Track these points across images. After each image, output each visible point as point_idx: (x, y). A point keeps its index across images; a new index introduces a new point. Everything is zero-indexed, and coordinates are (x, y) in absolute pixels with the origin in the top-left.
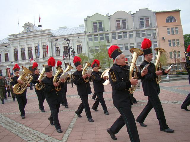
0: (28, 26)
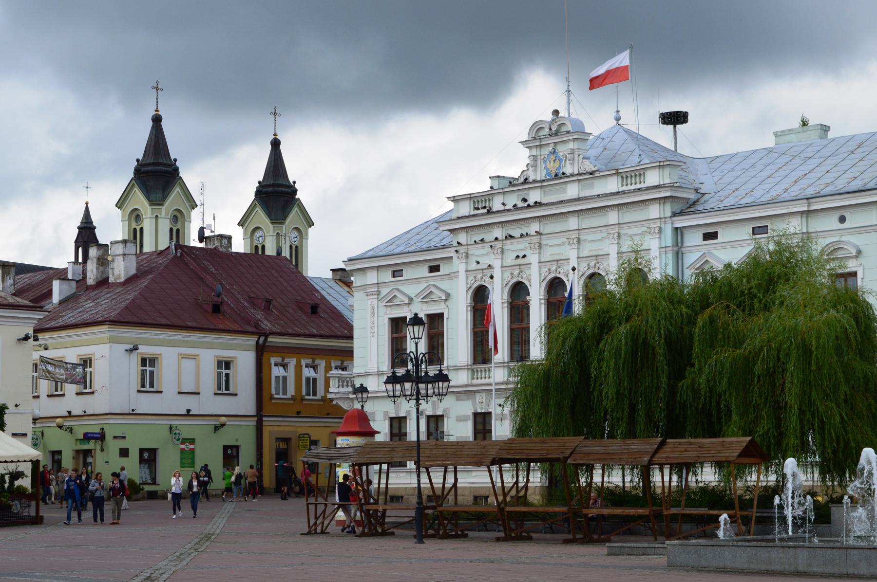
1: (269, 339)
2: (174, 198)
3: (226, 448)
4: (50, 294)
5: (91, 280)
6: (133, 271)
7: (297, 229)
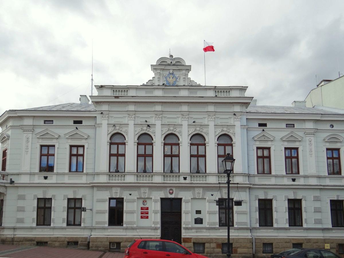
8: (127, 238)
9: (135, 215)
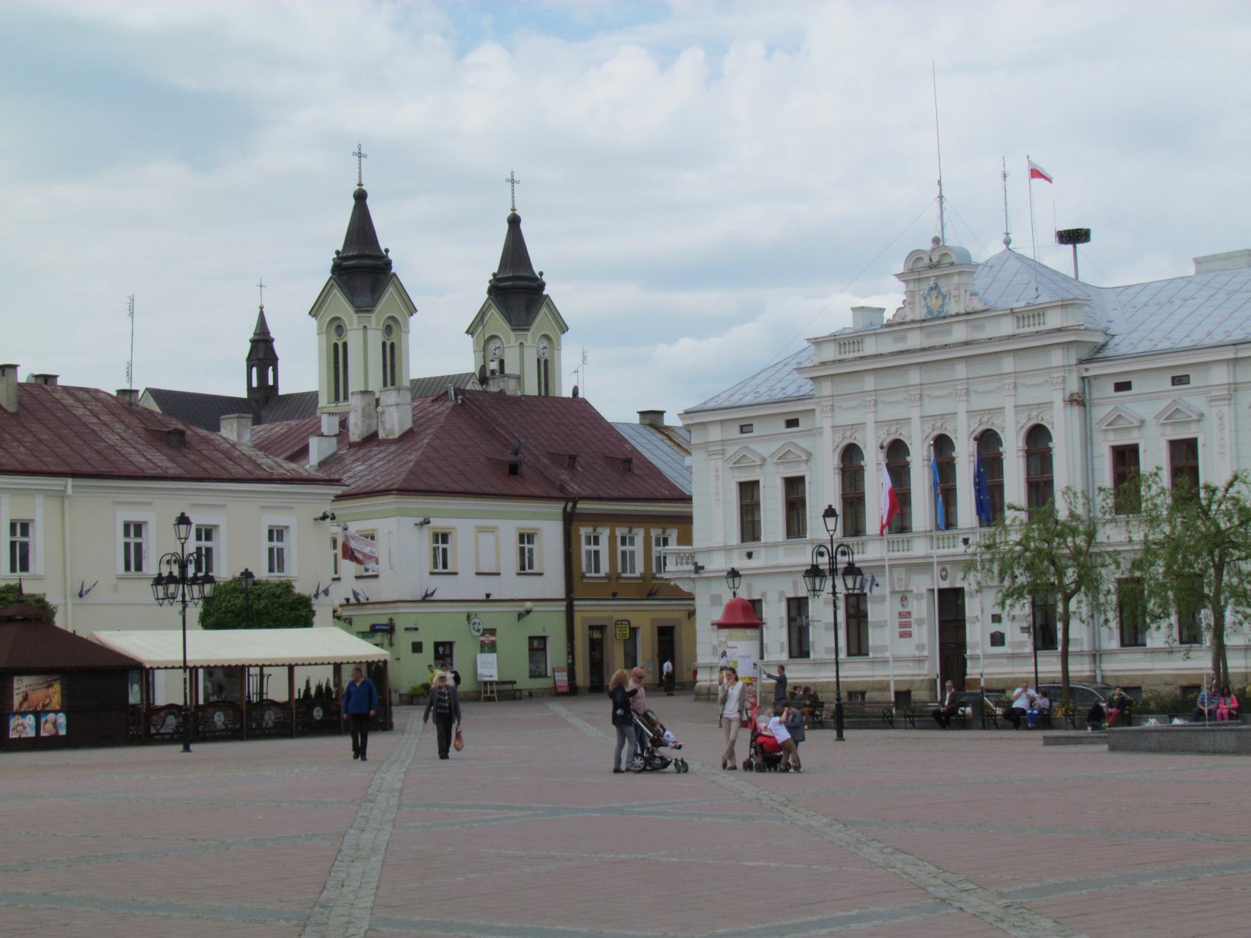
0: (933, 267)
1: (579, 506)
2: (388, 303)
3: (531, 639)
4: (303, 452)
5: (355, 434)
6: (408, 424)
7: (546, 337)
8: (874, 682)
9: (888, 630)
